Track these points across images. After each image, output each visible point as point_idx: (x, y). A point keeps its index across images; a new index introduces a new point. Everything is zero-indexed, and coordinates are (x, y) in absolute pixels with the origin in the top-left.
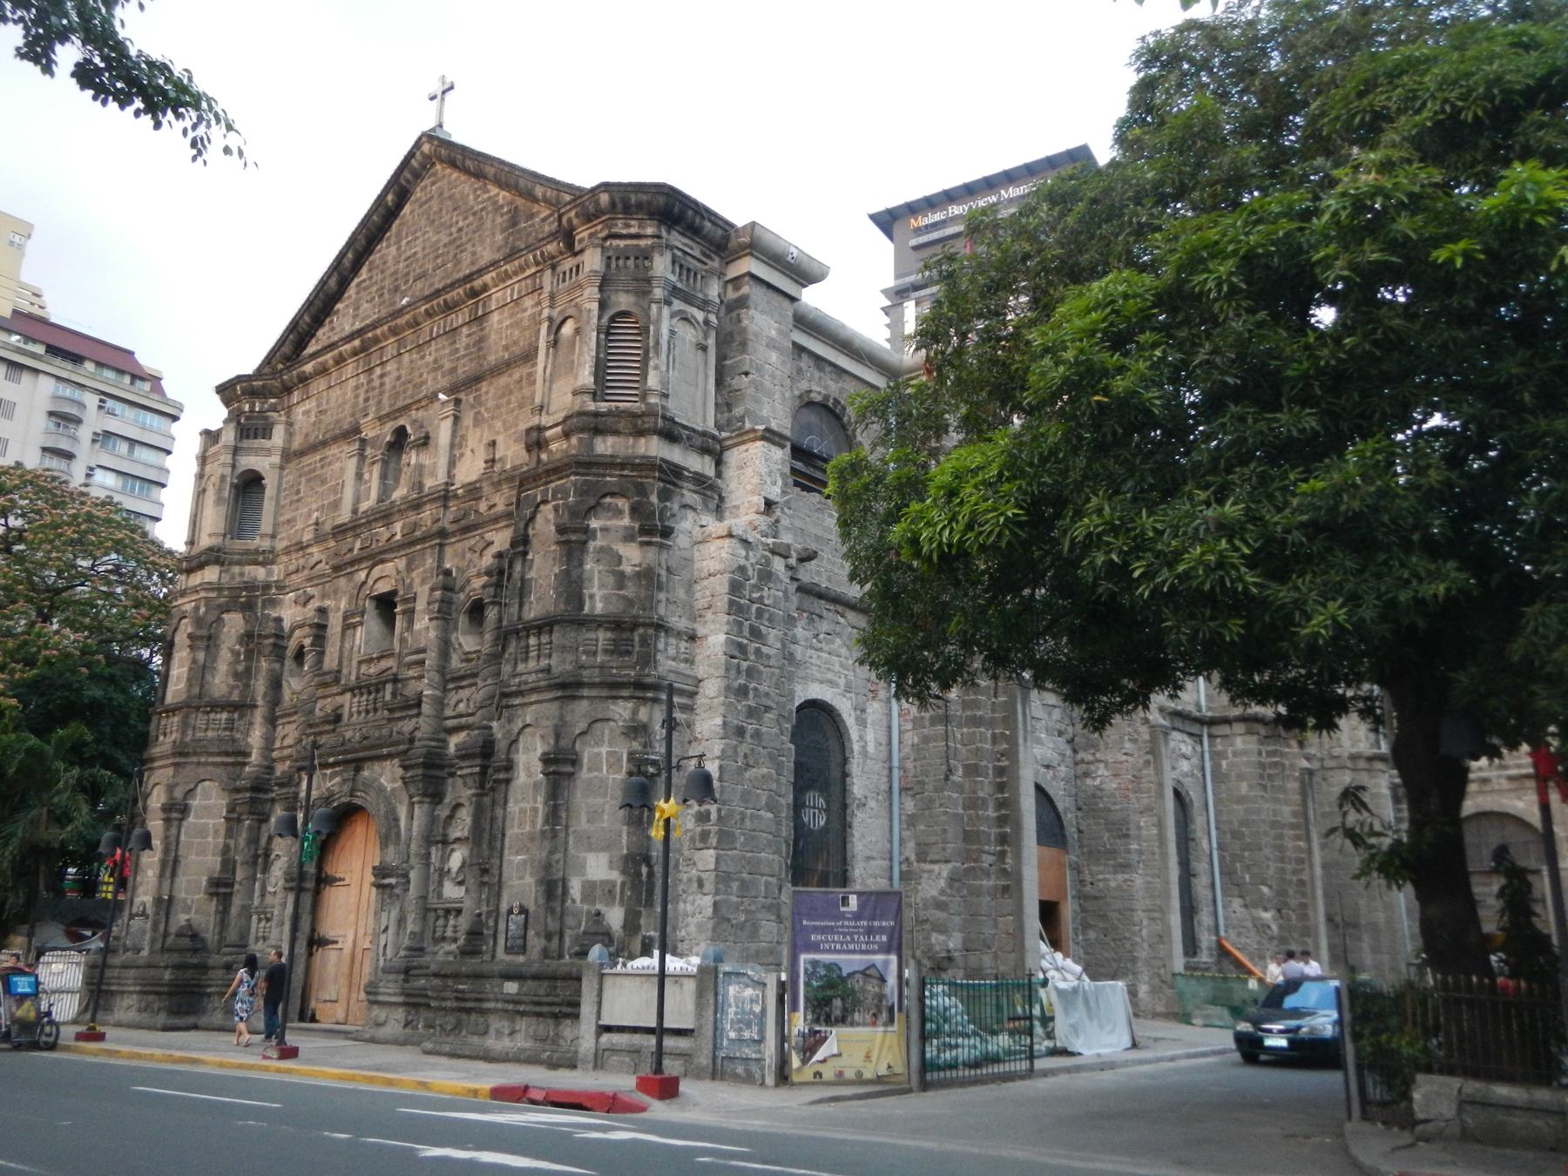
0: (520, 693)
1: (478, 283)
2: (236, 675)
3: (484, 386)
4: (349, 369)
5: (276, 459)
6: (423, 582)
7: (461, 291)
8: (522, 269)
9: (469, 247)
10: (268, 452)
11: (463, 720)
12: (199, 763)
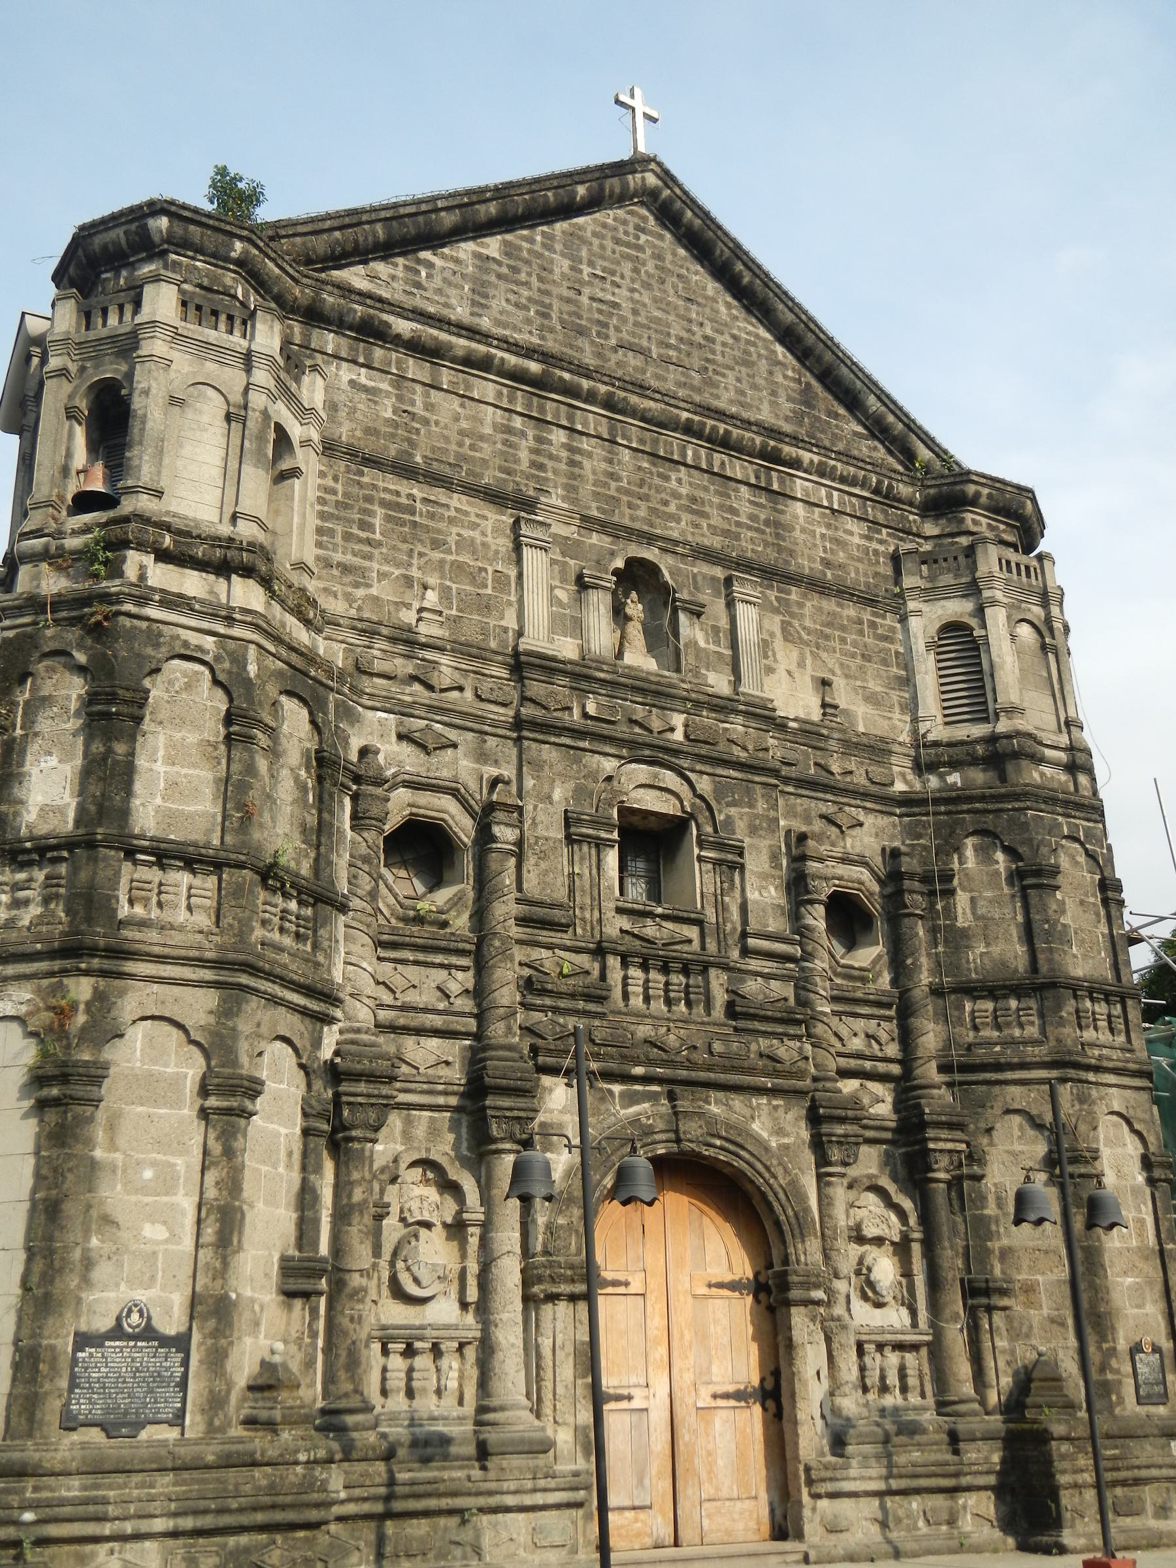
0: (1097, 1069)
1: (788, 450)
2: (304, 830)
3: (795, 594)
4: (486, 388)
5: (315, 436)
6: (753, 830)
7: (758, 440)
8: (853, 482)
9: (731, 376)
10: (304, 413)
11: (868, 1065)
12: (275, 1001)
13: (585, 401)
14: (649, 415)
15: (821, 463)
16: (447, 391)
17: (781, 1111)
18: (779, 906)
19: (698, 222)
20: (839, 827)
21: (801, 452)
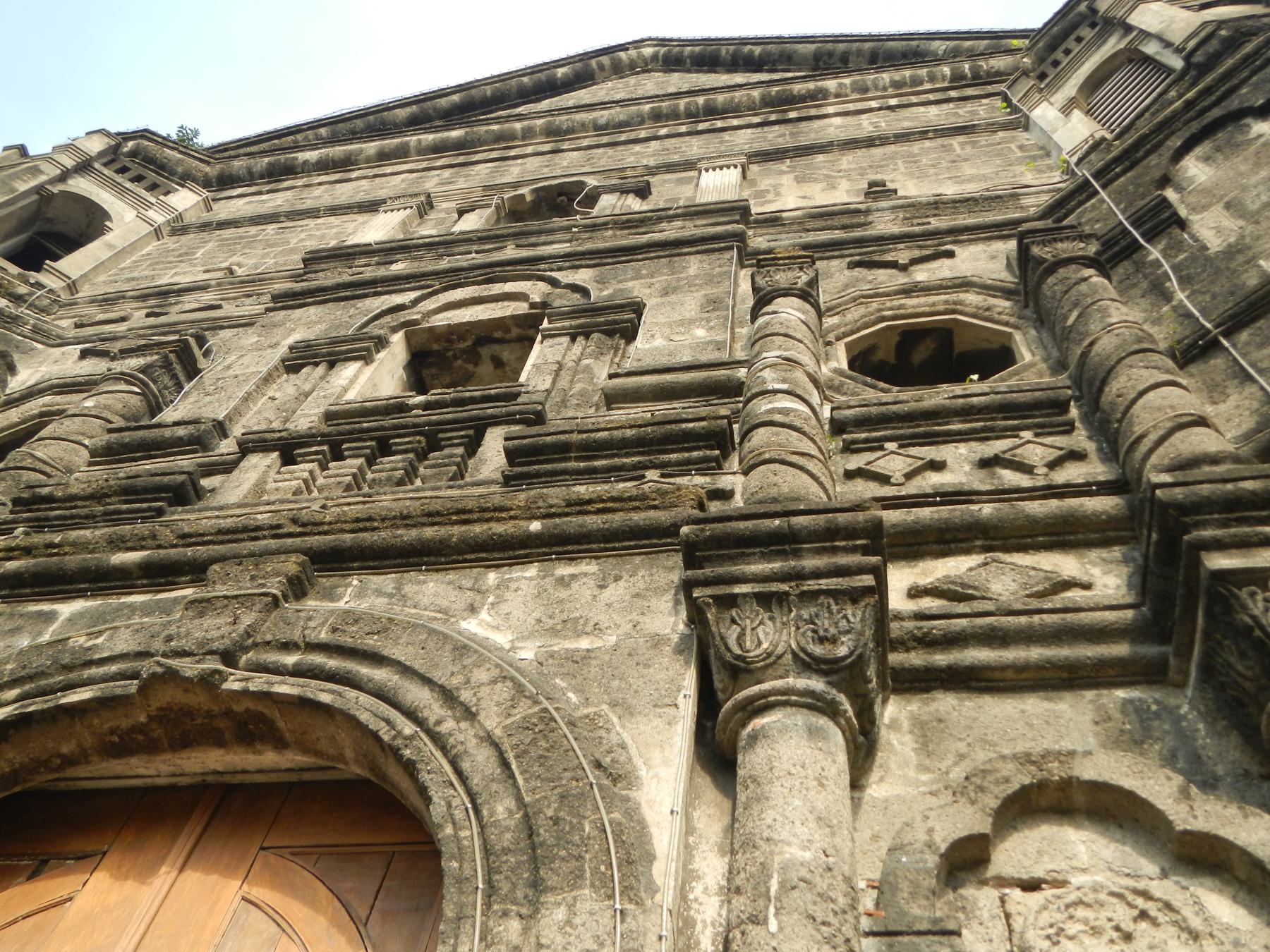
7: (756, 94)
13: (524, 138)
14: (602, 121)
15: (854, 83)
16: (357, 179)
17: (583, 591)
18: (710, 342)
19: (697, 49)
20: (893, 265)
21: (820, 84)
